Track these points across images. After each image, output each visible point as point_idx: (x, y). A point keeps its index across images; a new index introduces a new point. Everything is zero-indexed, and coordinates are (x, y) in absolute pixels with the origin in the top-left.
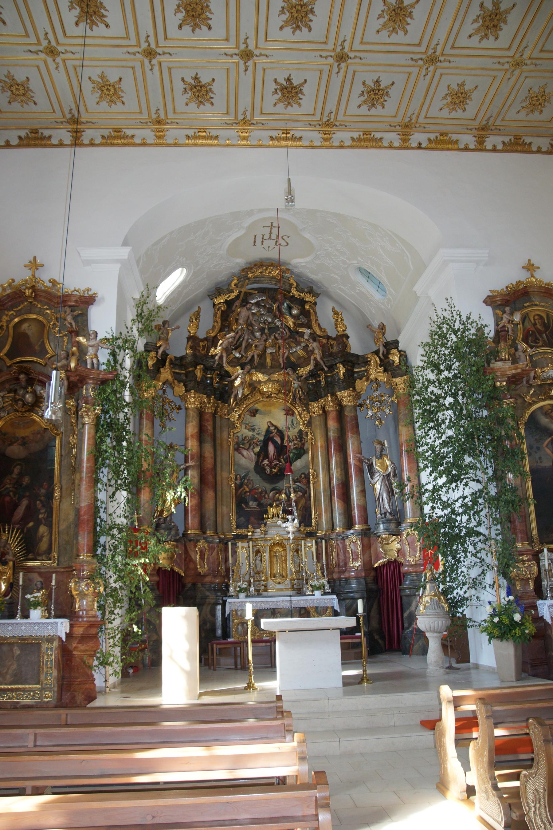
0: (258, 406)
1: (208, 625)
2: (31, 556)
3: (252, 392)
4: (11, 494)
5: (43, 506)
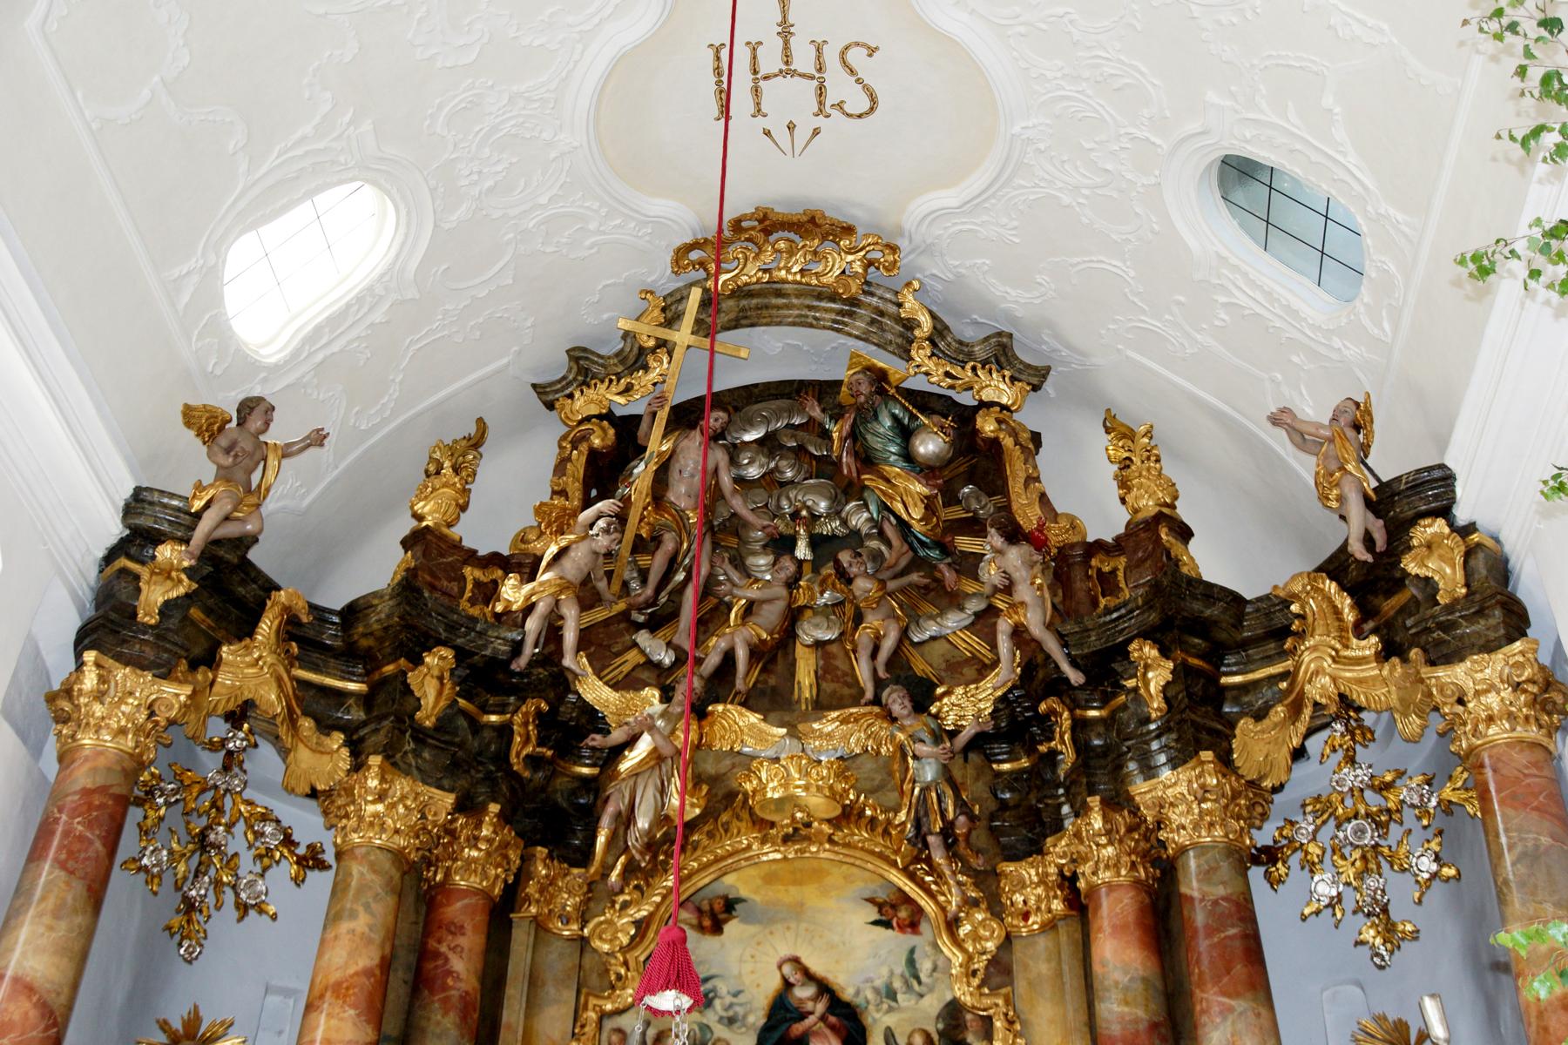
0: (735, 883)
3: (708, 814)
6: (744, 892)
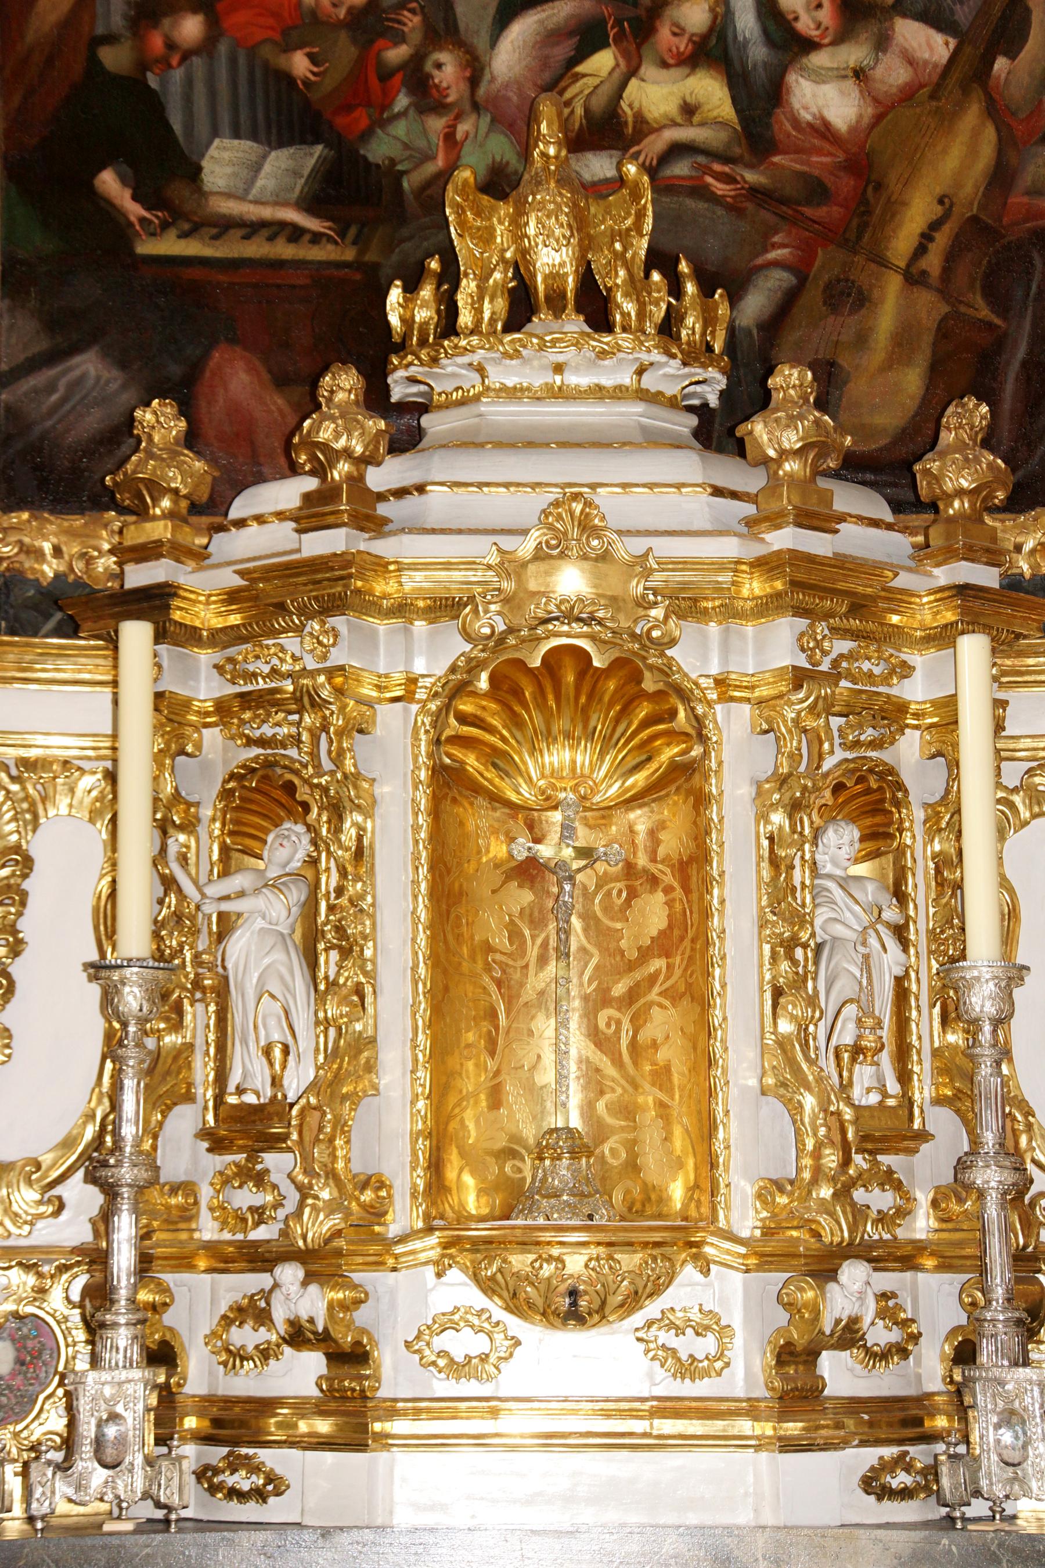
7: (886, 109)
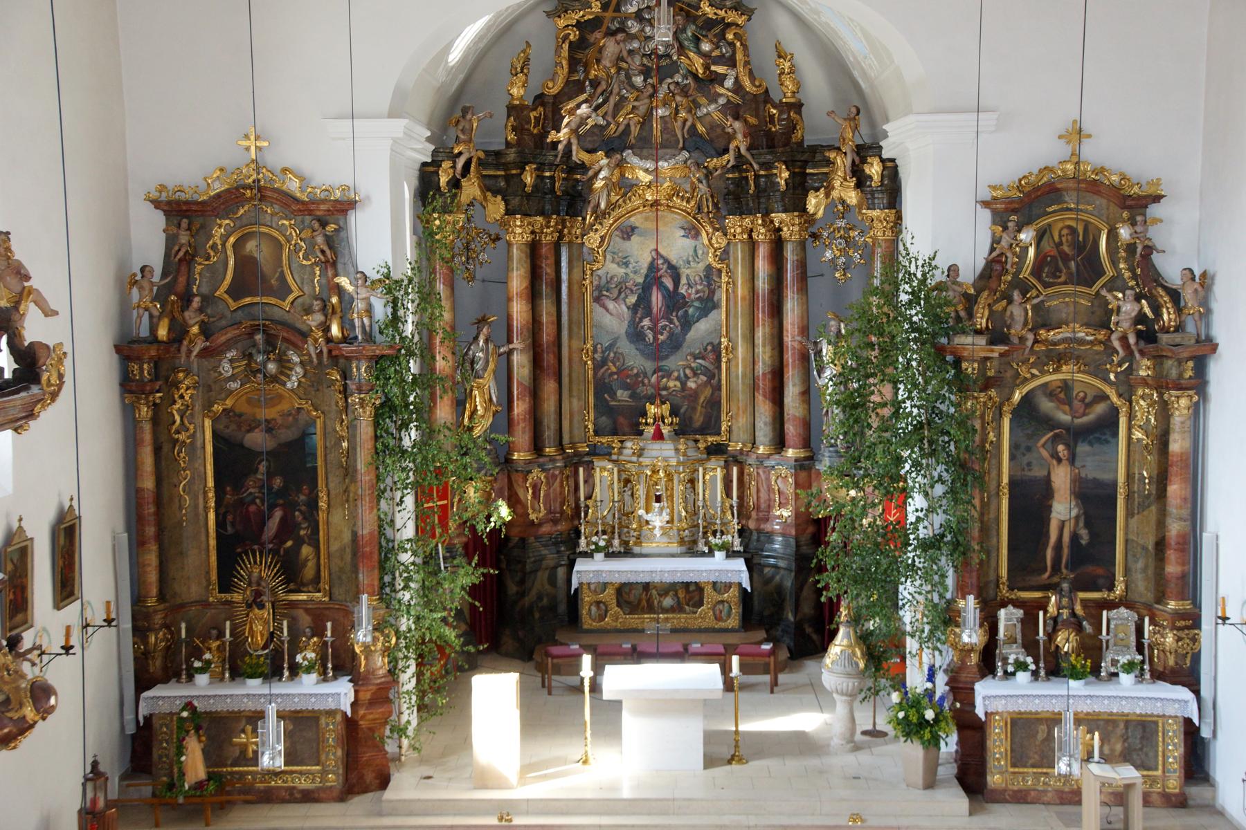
0: (635, 220)
1: (545, 600)
2: (292, 586)
4: (258, 501)
5: (305, 518)
6: (637, 225)
7: (699, 386)
